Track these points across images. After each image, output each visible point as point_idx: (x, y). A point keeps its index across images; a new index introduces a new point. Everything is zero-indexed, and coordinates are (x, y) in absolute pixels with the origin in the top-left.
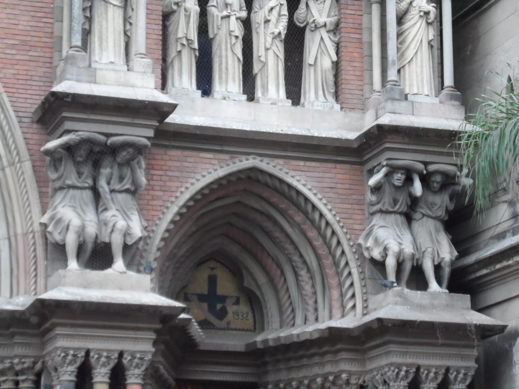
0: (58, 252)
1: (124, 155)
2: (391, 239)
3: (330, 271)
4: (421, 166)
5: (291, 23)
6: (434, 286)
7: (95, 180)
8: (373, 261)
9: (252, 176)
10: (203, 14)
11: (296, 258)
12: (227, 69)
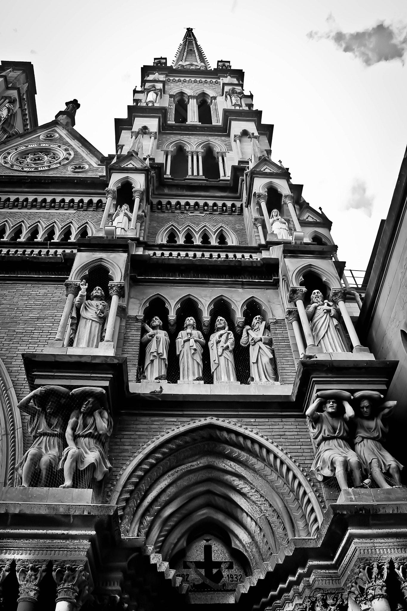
4: (347, 394)
12: (188, 369)
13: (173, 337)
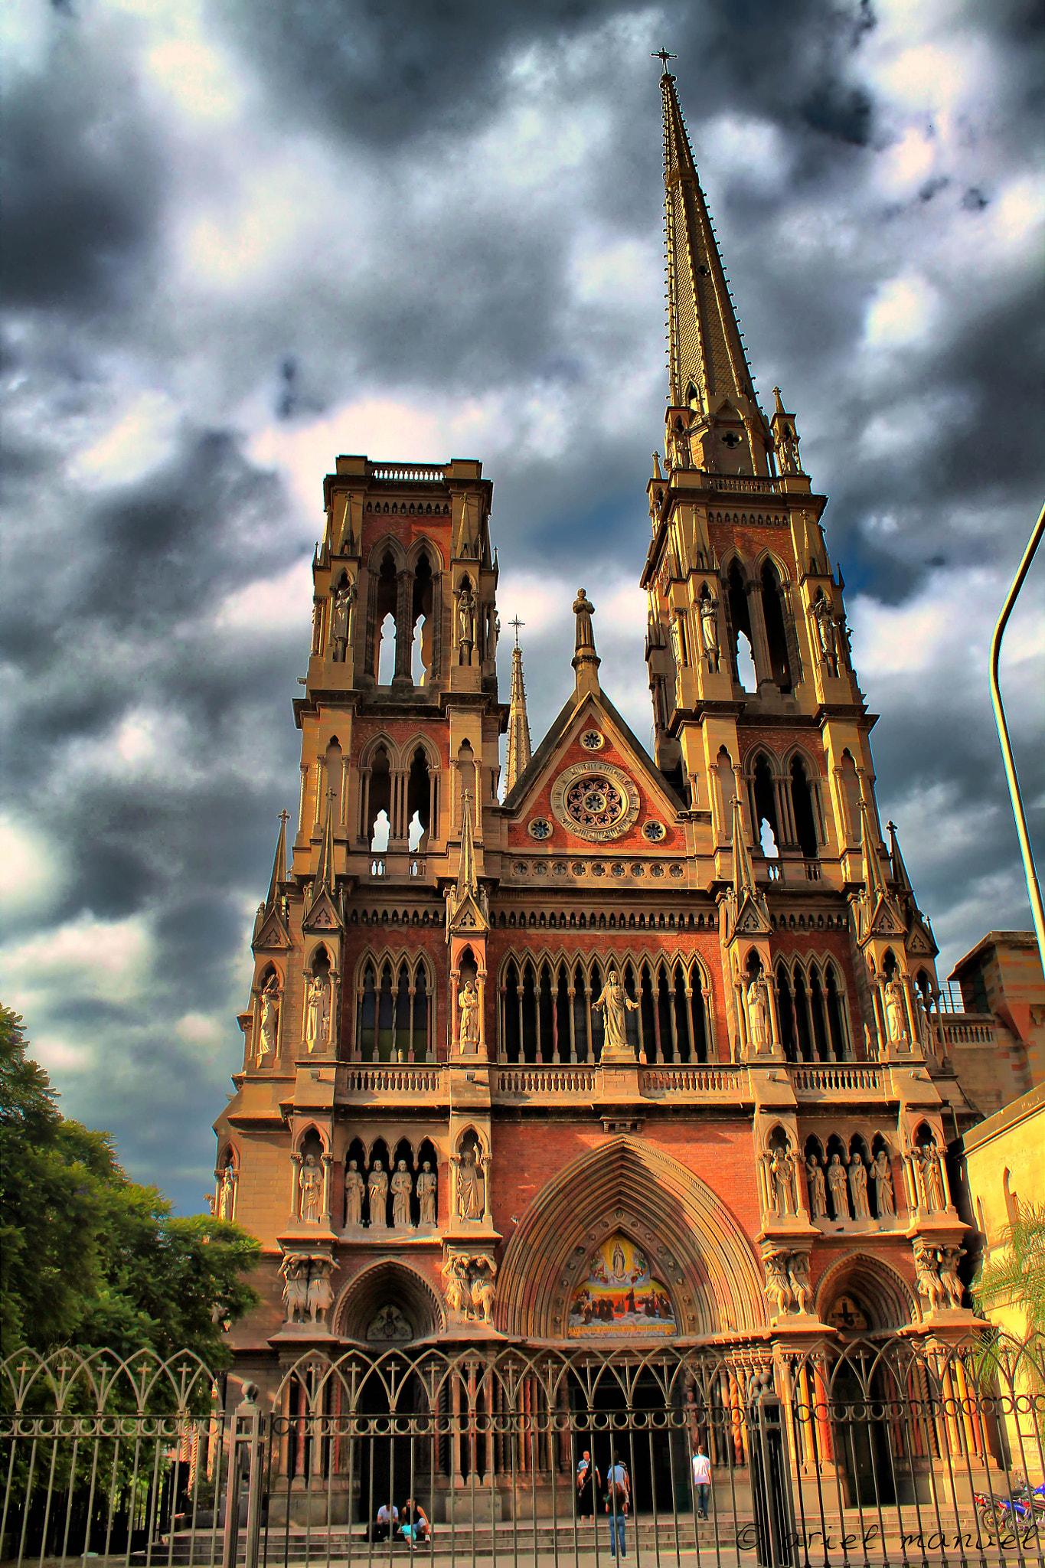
1: (799, 1258)
6: (953, 1306)
13: (825, 1173)
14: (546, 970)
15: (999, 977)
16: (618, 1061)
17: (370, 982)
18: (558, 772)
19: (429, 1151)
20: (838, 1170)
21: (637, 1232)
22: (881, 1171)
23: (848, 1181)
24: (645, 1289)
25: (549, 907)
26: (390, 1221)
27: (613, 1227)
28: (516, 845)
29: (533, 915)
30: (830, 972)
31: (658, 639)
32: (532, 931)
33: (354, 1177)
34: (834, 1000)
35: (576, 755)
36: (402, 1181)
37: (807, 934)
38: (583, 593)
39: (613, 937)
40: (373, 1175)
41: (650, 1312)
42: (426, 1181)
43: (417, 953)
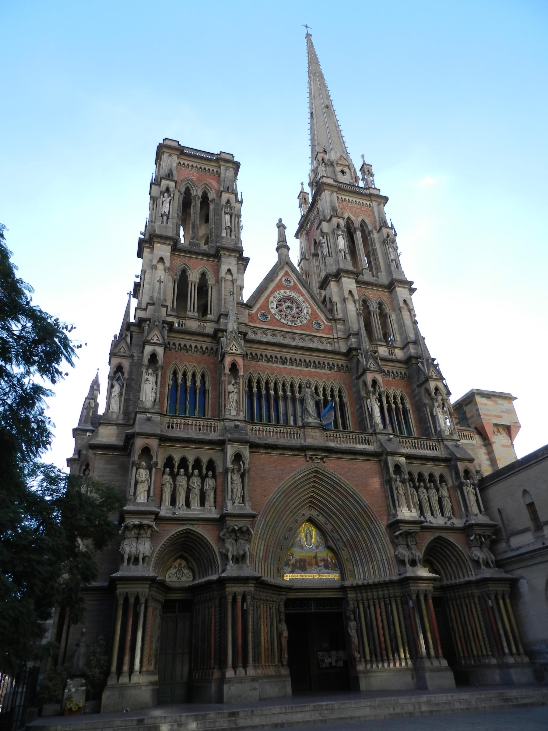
0: (401, 562)
2: (479, 554)
3: (462, 564)
5: (439, 497)
7: (407, 541)
8: (474, 560)
9: (439, 538)
10: (418, 495)
11: (450, 560)
13: (417, 492)
14: (267, 383)
15: (477, 410)
16: (312, 424)
17: (175, 379)
18: (272, 293)
19: (211, 465)
20: (422, 490)
21: (321, 519)
22: (444, 493)
23: (428, 497)
24: (324, 553)
25: (271, 351)
26: (188, 504)
27: (307, 516)
28: (252, 323)
29: (261, 355)
30: (402, 399)
31: (305, 256)
32: (260, 363)
33: (167, 478)
34: (405, 411)
35: (279, 286)
36: (196, 482)
37: (391, 379)
38: (280, 220)
39: (300, 370)
40: (179, 478)
41: (326, 567)
42: (210, 483)
43: (201, 367)
